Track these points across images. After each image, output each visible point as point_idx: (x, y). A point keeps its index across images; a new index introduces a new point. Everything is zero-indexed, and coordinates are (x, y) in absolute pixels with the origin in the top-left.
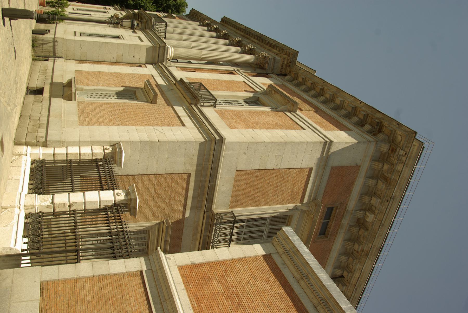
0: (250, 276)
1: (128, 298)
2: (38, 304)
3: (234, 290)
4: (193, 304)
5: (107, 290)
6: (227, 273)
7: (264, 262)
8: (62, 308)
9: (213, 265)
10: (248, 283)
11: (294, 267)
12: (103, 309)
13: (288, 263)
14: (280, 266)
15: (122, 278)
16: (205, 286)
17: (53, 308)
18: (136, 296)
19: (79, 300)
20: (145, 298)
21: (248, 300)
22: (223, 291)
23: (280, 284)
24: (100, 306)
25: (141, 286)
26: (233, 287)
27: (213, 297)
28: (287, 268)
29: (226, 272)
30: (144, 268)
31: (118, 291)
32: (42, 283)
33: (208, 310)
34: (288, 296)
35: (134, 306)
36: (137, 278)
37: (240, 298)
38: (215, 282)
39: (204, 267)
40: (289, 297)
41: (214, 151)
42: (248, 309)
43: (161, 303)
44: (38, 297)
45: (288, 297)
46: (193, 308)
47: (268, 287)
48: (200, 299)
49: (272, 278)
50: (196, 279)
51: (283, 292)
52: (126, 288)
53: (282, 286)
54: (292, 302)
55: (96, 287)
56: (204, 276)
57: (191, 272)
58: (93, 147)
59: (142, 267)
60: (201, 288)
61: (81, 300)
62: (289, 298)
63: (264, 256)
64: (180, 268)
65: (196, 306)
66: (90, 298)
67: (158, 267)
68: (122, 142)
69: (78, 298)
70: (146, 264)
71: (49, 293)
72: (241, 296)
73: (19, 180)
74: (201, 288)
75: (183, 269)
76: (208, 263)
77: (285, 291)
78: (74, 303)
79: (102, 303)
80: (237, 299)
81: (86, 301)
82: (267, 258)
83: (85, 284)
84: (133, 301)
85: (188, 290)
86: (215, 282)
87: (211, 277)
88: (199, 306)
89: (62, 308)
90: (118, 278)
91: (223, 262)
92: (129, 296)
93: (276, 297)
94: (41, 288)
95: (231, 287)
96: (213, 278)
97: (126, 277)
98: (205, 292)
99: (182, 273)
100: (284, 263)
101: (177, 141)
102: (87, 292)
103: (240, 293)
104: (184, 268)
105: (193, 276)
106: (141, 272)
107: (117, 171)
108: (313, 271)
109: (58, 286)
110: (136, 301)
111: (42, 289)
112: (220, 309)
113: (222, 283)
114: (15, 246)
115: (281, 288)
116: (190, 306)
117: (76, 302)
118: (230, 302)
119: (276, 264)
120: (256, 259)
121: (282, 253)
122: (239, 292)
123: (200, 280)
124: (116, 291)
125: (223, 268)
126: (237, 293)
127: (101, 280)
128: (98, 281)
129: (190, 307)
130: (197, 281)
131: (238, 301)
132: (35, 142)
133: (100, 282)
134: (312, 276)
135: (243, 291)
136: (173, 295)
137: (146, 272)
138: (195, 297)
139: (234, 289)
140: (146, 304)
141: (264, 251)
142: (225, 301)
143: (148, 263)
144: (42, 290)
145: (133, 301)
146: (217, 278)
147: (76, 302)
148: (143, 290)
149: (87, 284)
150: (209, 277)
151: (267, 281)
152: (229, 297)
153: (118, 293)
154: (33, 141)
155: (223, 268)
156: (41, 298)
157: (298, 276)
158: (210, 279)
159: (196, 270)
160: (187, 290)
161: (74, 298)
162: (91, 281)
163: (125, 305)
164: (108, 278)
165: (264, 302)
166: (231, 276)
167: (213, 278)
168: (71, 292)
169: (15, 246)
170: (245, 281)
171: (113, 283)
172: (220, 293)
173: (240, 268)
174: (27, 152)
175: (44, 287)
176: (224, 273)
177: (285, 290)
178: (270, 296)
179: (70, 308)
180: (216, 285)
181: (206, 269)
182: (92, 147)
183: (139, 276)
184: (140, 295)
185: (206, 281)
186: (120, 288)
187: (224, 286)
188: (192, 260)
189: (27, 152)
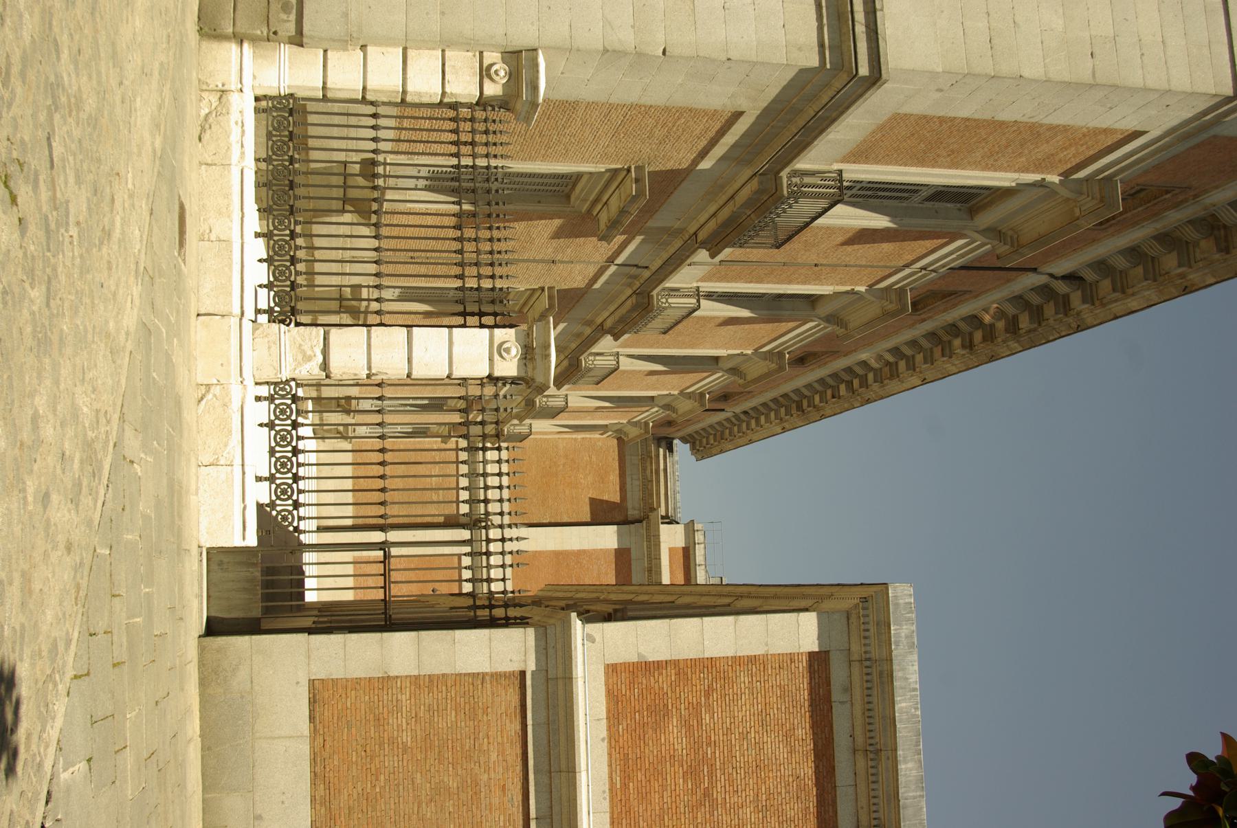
0: (756, 716)
1: (486, 748)
2: (305, 749)
3: (709, 752)
4: (614, 781)
5: (445, 720)
6: (711, 697)
7: (805, 673)
8: (354, 759)
9: (685, 669)
10: (744, 736)
11: (864, 713)
12: (432, 770)
13: (857, 693)
14: (836, 695)
15: (480, 686)
16: (650, 731)
17: (336, 757)
18: (503, 743)
19: (386, 741)
20: (519, 751)
21: (727, 786)
22: (684, 751)
23: (814, 750)
24: (428, 761)
25: (516, 717)
26: (709, 744)
27: (660, 768)
28: (848, 705)
29: (707, 695)
30: (531, 666)
31: (468, 723)
32: (312, 682)
33: (640, 802)
34: (816, 786)
35: (495, 771)
36: (511, 690)
37: (714, 778)
38: (675, 724)
39: (664, 671)
40: (817, 790)
41: (838, 92)
42: (720, 810)
43: (550, 772)
44: (305, 727)
45: (815, 789)
46: (611, 790)
47: (783, 753)
48: (631, 768)
49: (803, 731)
50: (637, 708)
51: (810, 773)
52: (485, 716)
53: (815, 757)
54: (817, 807)
55: (422, 707)
56: (657, 702)
57: (632, 685)
58: (448, 53)
59: (525, 661)
60: (642, 738)
61: (392, 741)
62: (815, 793)
63: (811, 655)
64: (610, 670)
65: (618, 787)
66: (409, 739)
67: (560, 674)
68: (547, 49)
69: (386, 735)
70: (537, 652)
71: (326, 714)
72: (718, 771)
73: (228, 242)
74: (642, 738)
75: (615, 674)
76: (676, 663)
77: (815, 772)
78: (377, 746)
79: (433, 754)
80: (706, 778)
81: (400, 746)
82: (818, 662)
83: (399, 697)
84: (494, 756)
85: (613, 740)
86: (675, 724)
87: (670, 708)
88: (625, 786)
89: (354, 759)
90: (471, 686)
91: (707, 665)
92: (489, 743)
93: (791, 785)
94: (311, 696)
95: (705, 744)
96: (674, 710)
97: (489, 686)
98: (647, 751)
99: (611, 687)
100: (848, 689)
101: (725, 59)
102: (404, 720)
103: (718, 763)
104: (619, 669)
105: (632, 697)
106: (523, 674)
107: (510, 245)
108: (896, 750)
109: (344, 696)
110: (500, 757)
111: (312, 700)
112: (665, 801)
113: (689, 728)
114: (244, 539)
115: (810, 762)
116: (607, 788)
117: (381, 745)
118: (690, 786)
119: (829, 684)
120: (789, 662)
121: (855, 657)
122: (718, 760)
123: (645, 713)
124: (463, 724)
125: (706, 681)
126: (714, 762)
127: (435, 689)
128: (426, 689)
129: (604, 792)
130: (637, 714)
131: (706, 785)
132: (265, 33)
133: (431, 694)
134: (888, 758)
135: (726, 759)
136: (577, 770)
137: (532, 675)
138: (622, 762)
139: (709, 749)
140: (519, 768)
141: (818, 639)
142: (681, 780)
143: (543, 650)
144: (313, 701)
145: (494, 756)
146: (683, 713)
147: (381, 745)
148: (518, 727)
149: (404, 696)
150: (666, 706)
151: (788, 735)
152: (692, 772)
153: (467, 729)
154: (259, 32)
155: (706, 681)
156: (312, 725)
157: (860, 740)
158: (667, 714)
159: (644, 682)
160: (610, 742)
161: (377, 734)
162: (413, 687)
163: (477, 764)
164: (449, 685)
165: (760, 795)
166: (716, 710)
167: (674, 710)
168: (372, 716)
169: (244, 539)
170: (741, 731)
171: (458, 699)
172: (676, 759)
173: (743, 685)
174: (241, 83)
175: (318, 693)
176: (703, 699)
177: (817, 767)
178: (779, 780)
179: (368, 760)
180: (675, 736)
181: (664, 681)
182: (443, 51)
183: (517, 682)
184: (512, 742)
185: (658, 718)
186: (472, 718)
187: (692, 739)
188: (642, 650)
189: (241, 83)
